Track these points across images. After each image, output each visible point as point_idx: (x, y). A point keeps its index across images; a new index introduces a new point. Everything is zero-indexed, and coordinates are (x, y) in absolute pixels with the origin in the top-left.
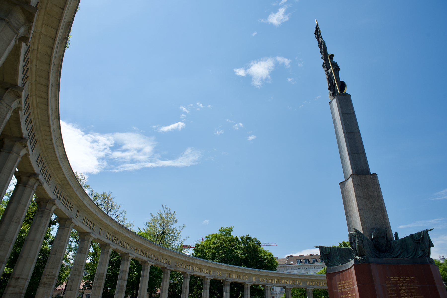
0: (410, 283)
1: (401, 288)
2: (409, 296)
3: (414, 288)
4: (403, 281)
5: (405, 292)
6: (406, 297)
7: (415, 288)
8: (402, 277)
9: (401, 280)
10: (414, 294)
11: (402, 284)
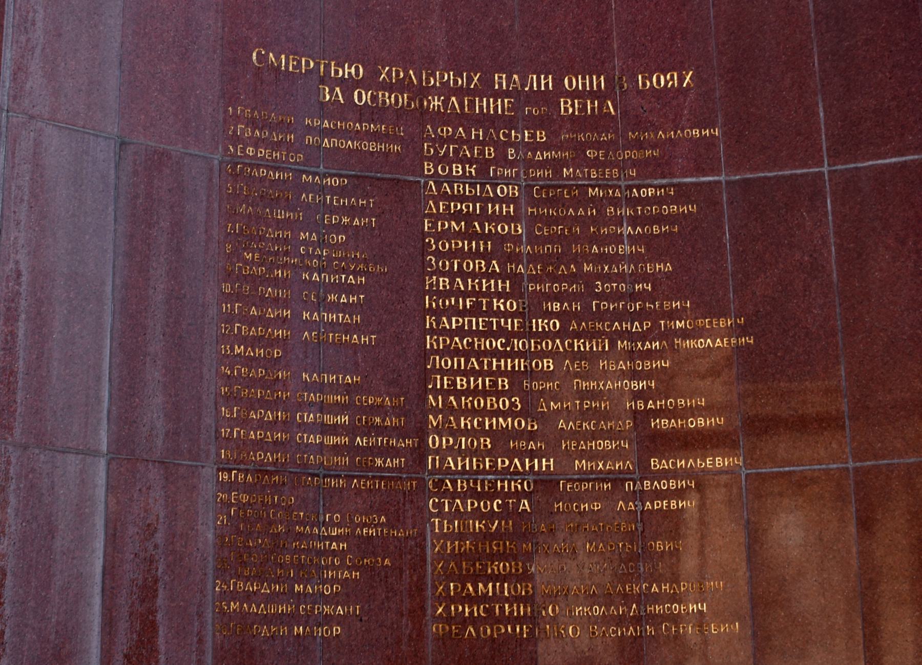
0: (598, 145)
1: (458, 216)
2: (539, 324)
3: (634, 221)
4: (510, 123)
5: (489, 275)
6: (501, 332)
7: (659, 219)
8: (500, 80)
9: (484, 105)
10: (616, 296)
11: (483, 165)
